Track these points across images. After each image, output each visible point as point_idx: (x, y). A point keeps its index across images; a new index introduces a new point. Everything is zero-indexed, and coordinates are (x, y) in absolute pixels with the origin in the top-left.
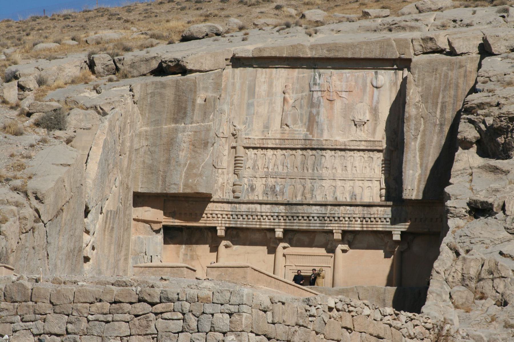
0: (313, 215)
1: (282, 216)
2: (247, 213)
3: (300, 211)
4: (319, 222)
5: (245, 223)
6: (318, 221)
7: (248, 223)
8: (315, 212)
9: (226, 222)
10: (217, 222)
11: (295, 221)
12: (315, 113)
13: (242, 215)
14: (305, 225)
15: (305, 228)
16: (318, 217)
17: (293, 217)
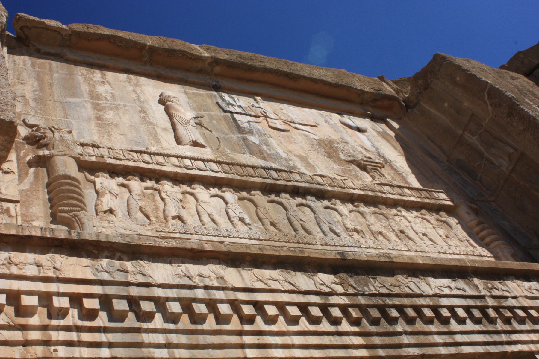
0: (445, 301)
1: (344, 308)
2: (186, 293)
3: (396, 290)
4: (477, 327)
5: (183, 339)
6: (470, 326)
7: (202, 339)
8: (447, 291)
9: (73, 336)
10: (17, 336)
11: (399, 328)
12: (257, 143)
13: (160, 304)
14: (438, 339)
15: (443, 351)
16: (467, 309)
17: (382, 309)
